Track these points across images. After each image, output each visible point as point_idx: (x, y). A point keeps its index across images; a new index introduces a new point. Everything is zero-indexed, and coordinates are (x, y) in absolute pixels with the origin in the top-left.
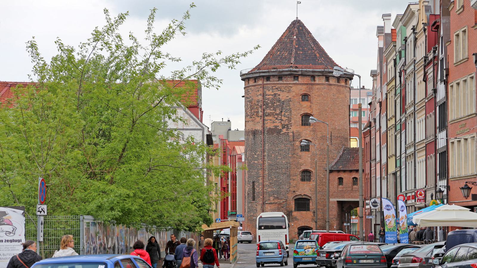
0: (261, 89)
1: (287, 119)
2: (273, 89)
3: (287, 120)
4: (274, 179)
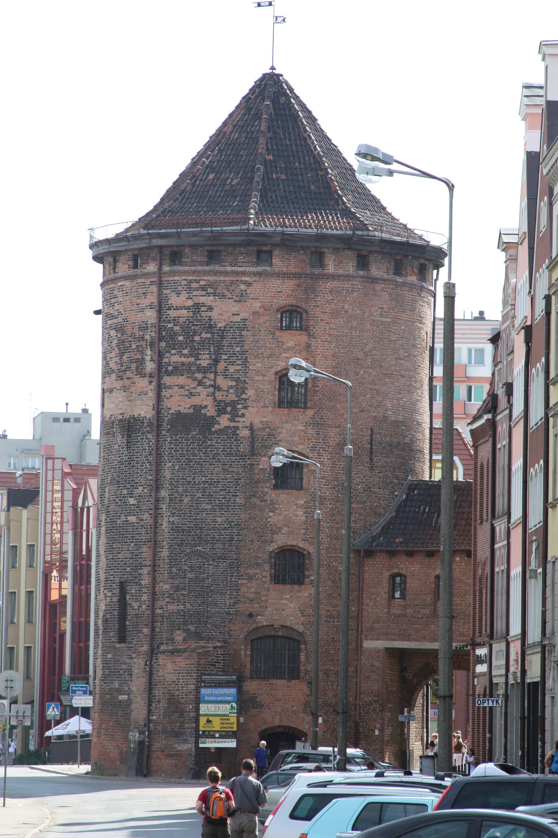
0: (154, 288)
1: (234, 383)
2: (190, 289)
3: (232, 387)
4: (189, 575)
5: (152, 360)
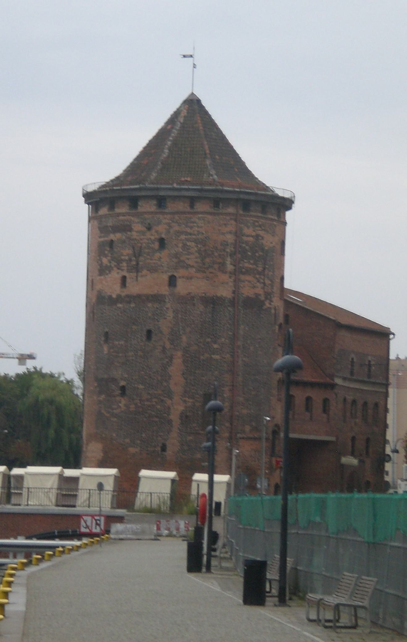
5: (231, 264)
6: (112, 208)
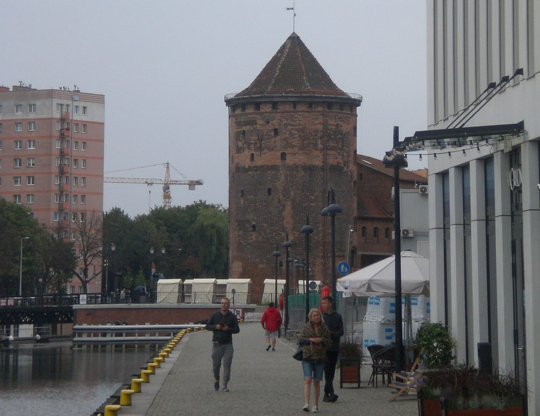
6: (244, 109)
